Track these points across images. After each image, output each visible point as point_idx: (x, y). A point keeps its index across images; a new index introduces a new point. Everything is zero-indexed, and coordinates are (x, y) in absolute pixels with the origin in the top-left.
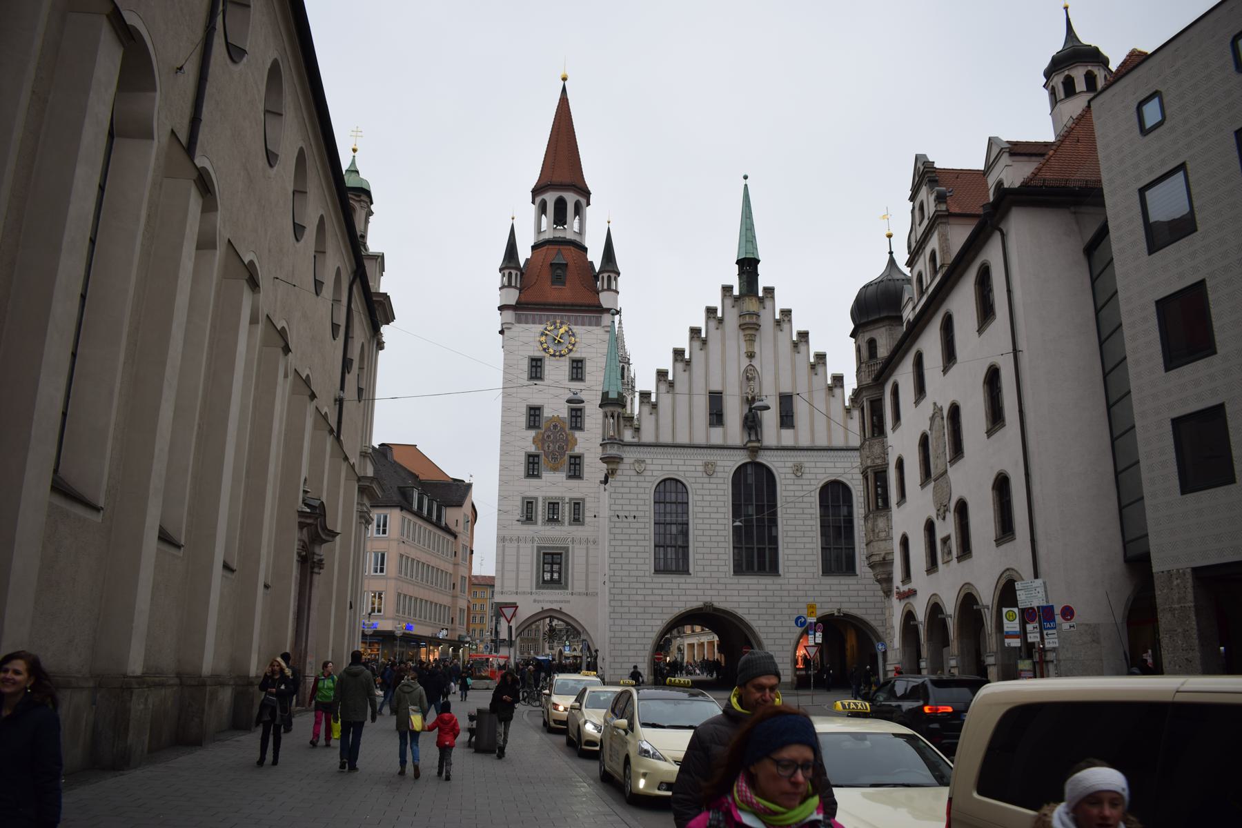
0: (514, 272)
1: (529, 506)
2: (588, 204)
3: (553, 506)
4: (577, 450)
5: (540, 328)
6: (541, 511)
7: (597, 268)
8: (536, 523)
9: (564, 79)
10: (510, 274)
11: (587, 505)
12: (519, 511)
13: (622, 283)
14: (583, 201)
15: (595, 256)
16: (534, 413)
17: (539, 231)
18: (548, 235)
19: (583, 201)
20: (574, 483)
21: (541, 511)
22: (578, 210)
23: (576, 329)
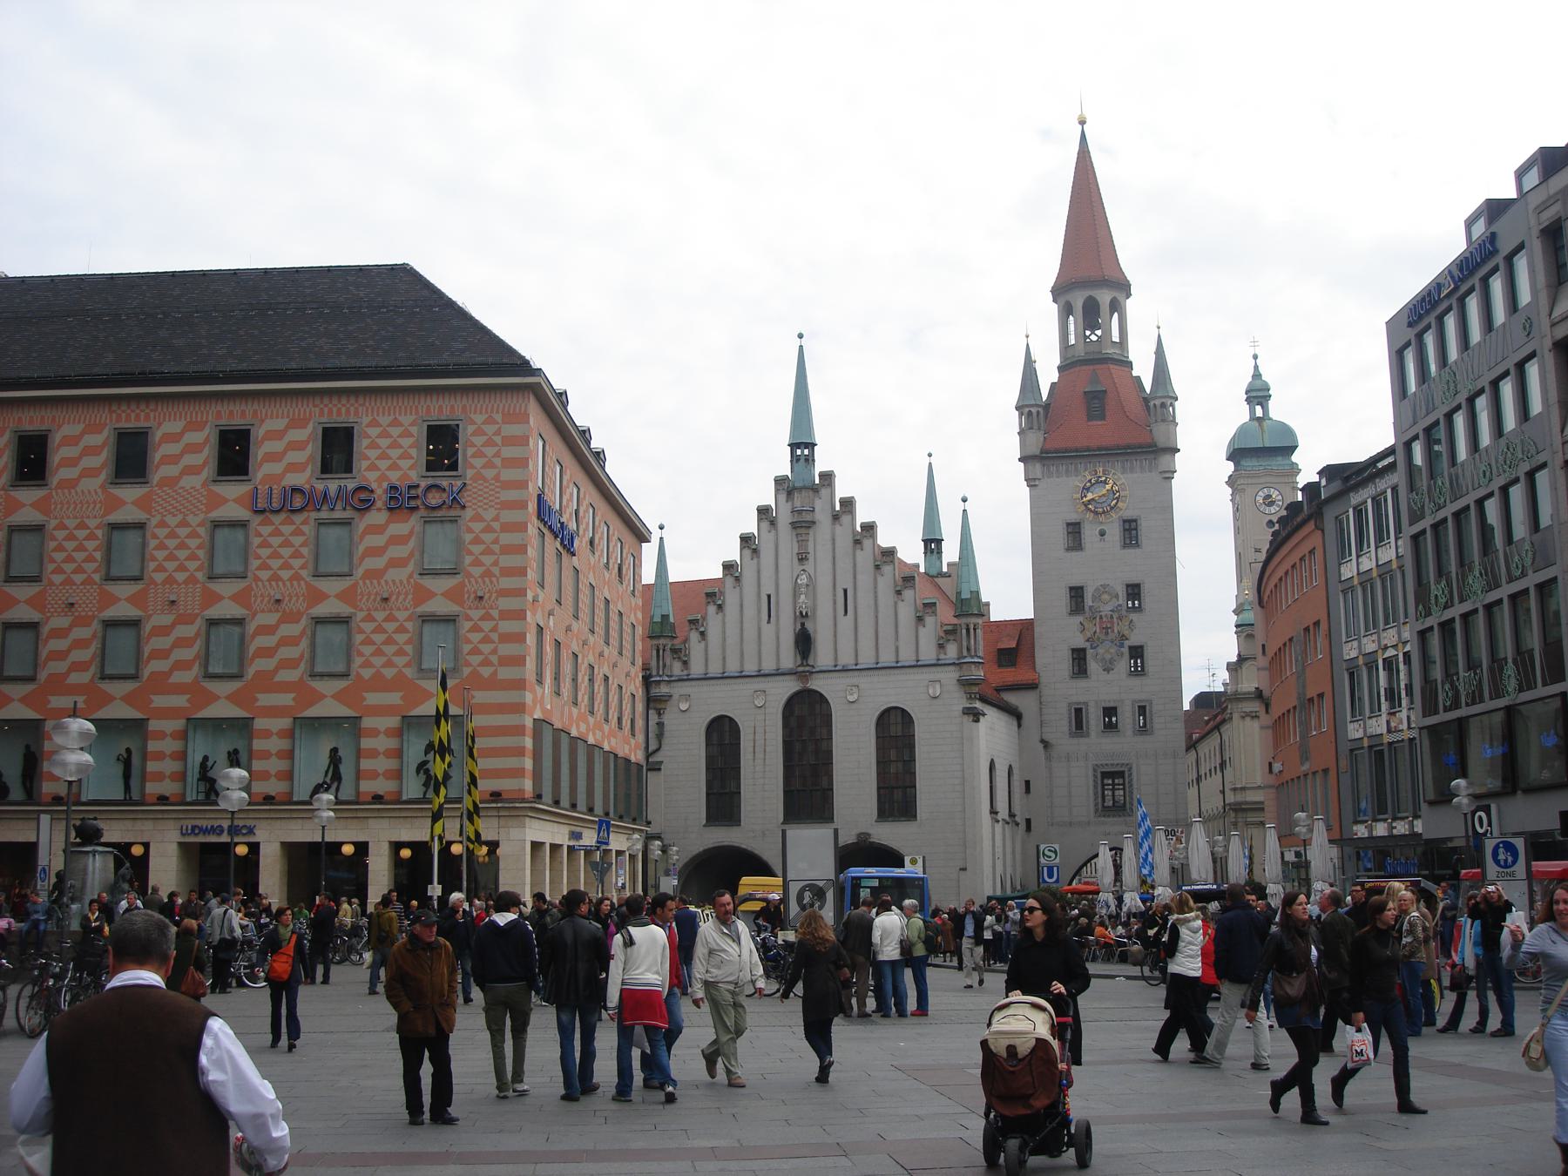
0: (1034, 410)
1: (1079, 715)
2: (1129, 295)
3: (1110, 712)
4: (1135, 640)
5: (1077, 482)
6: (1094, 719)
7: (1148, 385)
8: (1088, 735)
9: (1082, 122)
10: (1030, 413)
11: (1155, 708)
12: (1065, 722)
13: (1181, 410)
14: (1120, 297)
15: (1143, 369)
16: (1077, 593)
17: (1065, 346)
18: (1081, 352)
19: (1120, 297)
20: (1136, 681)
21: (1094, 719)
22: (1116, 306)
23: (1123, 479)
